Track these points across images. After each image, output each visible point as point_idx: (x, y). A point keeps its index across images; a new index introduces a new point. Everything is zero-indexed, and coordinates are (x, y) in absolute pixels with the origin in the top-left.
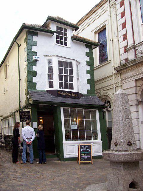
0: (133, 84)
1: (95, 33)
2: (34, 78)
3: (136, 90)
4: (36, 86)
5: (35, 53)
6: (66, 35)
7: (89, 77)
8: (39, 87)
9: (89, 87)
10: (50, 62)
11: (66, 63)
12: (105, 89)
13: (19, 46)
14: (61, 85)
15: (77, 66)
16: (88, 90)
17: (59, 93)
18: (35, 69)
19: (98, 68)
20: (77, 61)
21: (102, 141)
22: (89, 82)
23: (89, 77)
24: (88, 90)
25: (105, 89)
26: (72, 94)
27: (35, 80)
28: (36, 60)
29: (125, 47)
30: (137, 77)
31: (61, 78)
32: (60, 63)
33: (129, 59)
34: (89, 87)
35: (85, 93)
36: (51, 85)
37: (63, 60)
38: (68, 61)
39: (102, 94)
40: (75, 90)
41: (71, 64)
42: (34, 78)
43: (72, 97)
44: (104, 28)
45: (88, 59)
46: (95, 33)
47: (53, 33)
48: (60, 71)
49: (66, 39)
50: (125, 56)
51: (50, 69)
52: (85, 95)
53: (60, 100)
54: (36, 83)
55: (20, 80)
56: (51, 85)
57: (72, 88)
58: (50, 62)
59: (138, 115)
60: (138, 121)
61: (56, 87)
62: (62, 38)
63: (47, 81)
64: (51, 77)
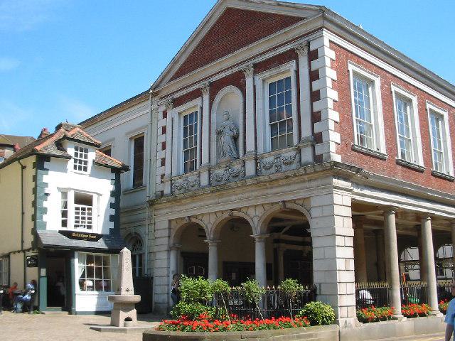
0: (166, 225)
1: (131, 139)
2: (44, 216)
3: (170, 232)
4: (45, 225)
5: (46, 185)
6: (86, 157)
9: (112, 225)
12: (136, 224)
13: (24, 168)
15: (98, 199)
17: (74, 234)
19: (128, 192)
20: (97, 194)
21: (138, 298)
25: (136, 224)
28: (47, 194)
29: (163, 176)
30: (171, 218)
33: (165, 192)
36: (64, 224)
39: (133, 231)
42: (44, 216)
43: (88, 239)
44: (142, 135)
46: (131, 139)
47: (70, 158)
49: (86, 163)
50: (160, 188)
53: (74, 243)
55: (23, 213)
56: (64, 224)
57: (89, 227)
59: (169, 263)
60: (168, 271)
62: (81, 162)
63: (60, 219)
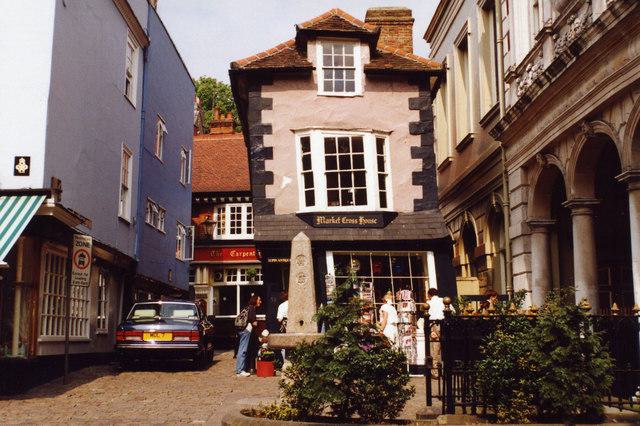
5: (268, 129)
6: (350, 61)
7: (418, 165)
8: (281, 208)
9: (418, 192)
10: (306, 143)
11: (344, 142)
14: (332, 198)
15: (380, 144)
16: (416, 201)
18: (269, 165)
22: (417, 178)
23: (418, 165)
24: (416, 201)
26: (361, 219)
27: (270, 192)
31: (331, 180)
32: (329, 144)
34: (418, 192)
35: (408, 208)
36: (310, 199)
37: (337, 135)
38: (350, 135)
40: (373, 204)
41: (358, 144)
45: (415, 116)
48: (330, 163)
51: (307, 162)
52: (407, 215)
54: (413, 158)
56: (310, 199)
57: (362, 198)
58: (306, 143)
61: (321, 204)
64: (309, 180)
